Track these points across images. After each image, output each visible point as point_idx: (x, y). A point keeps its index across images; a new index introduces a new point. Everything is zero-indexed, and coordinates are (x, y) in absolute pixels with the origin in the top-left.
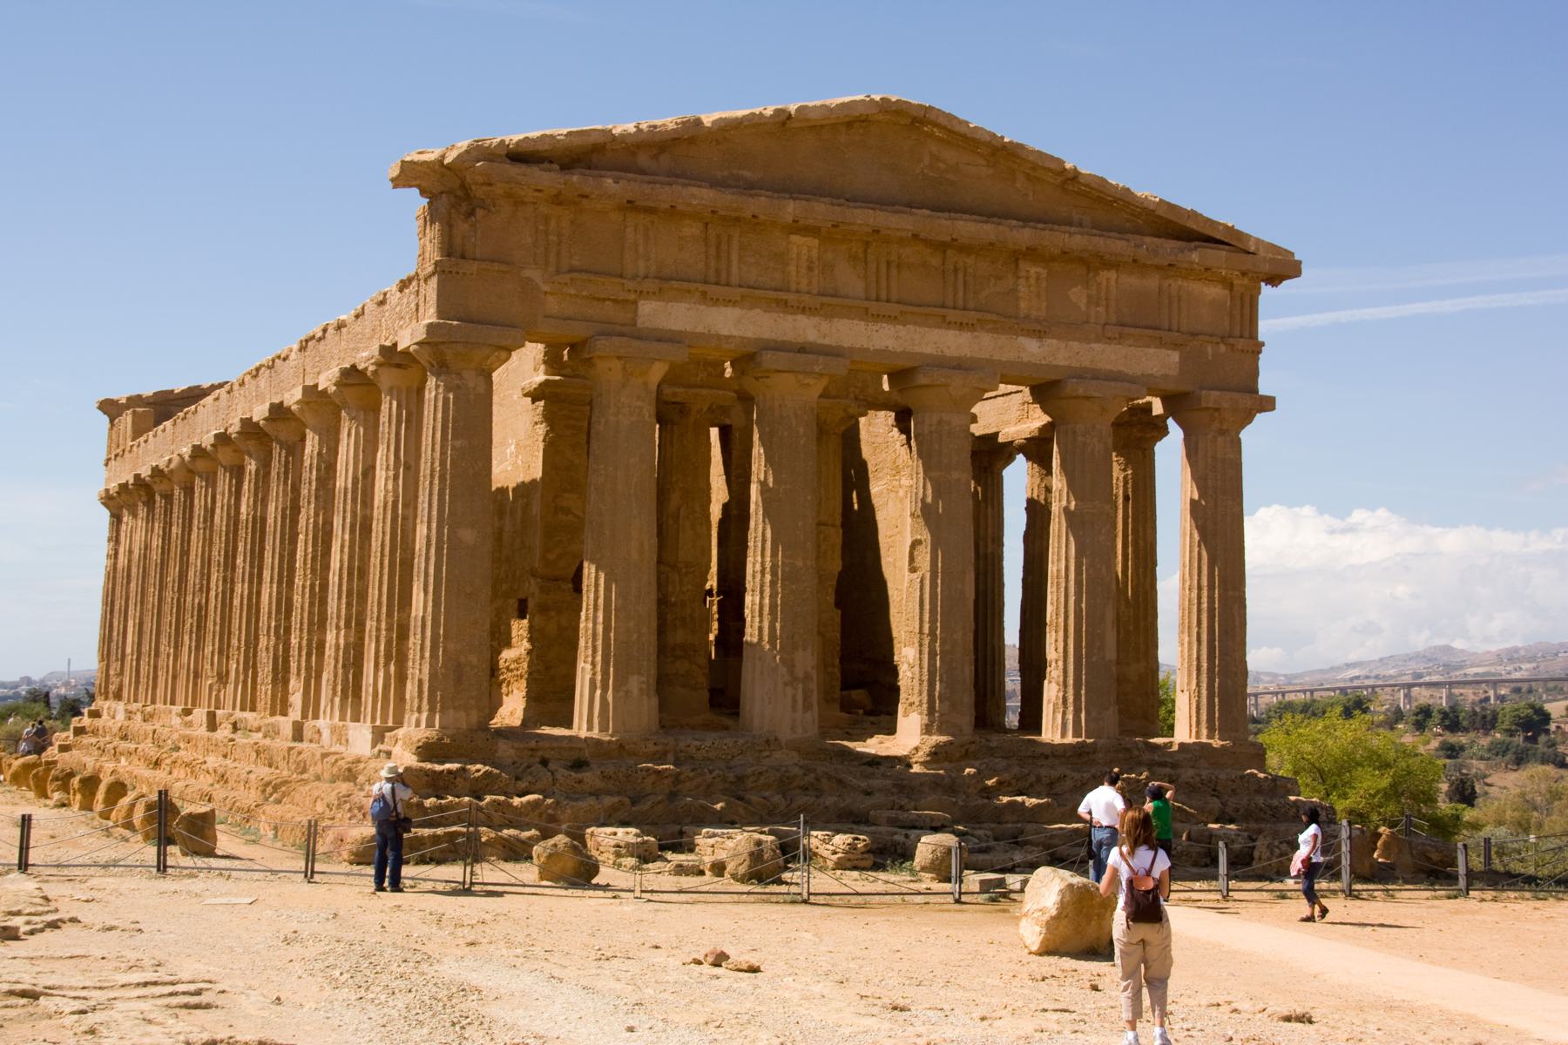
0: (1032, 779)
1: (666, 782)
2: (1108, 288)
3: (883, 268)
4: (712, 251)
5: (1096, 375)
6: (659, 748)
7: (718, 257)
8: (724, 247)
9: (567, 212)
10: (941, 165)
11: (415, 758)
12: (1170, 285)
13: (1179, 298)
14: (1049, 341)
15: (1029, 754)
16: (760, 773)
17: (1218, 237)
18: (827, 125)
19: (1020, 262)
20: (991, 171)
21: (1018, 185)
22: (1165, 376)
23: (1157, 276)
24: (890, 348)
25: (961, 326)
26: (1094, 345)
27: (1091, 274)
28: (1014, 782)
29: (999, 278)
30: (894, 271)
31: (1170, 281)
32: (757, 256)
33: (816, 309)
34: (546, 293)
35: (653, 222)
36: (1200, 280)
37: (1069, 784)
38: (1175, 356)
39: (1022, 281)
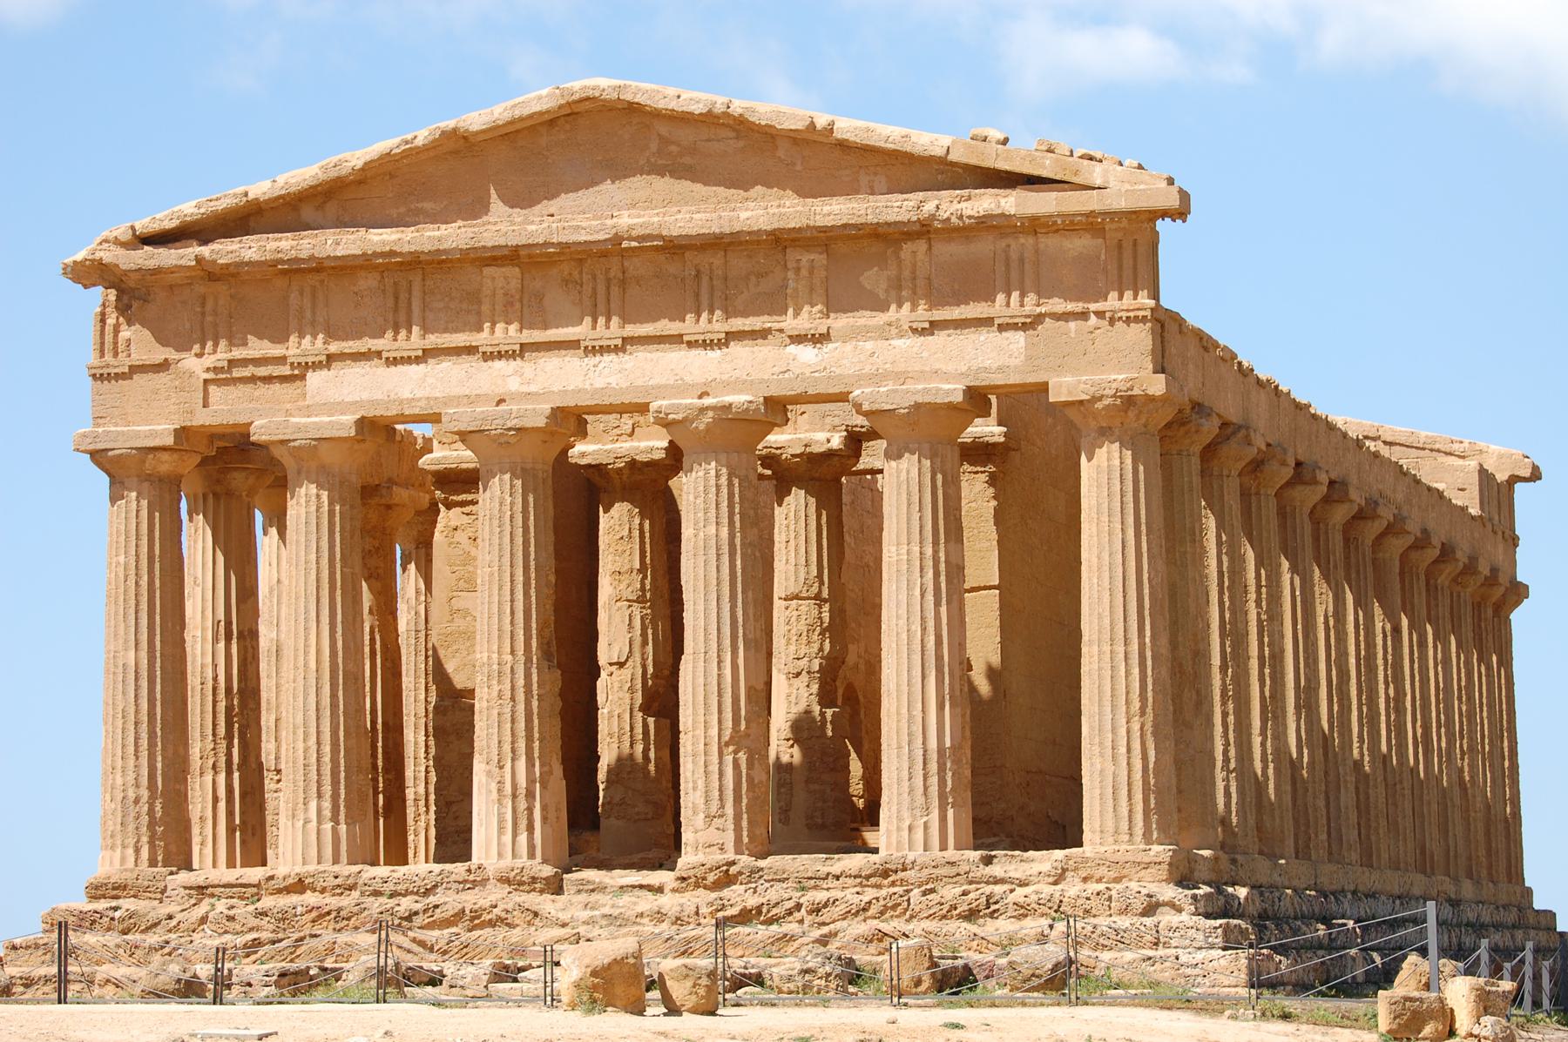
0: (789, 905)
1: (328, 918)
2: (914, 265)
3: (601, 289)
4: (390, 302)
5: (903, 377)
7: (396, 310)
8: (403, 296)
9: (225, 288)
10: (673, 148)
11: (86, 900)
12: (1009, 246)
13: (1022, 260)
14: (831, 346)
15: (810, 874)
16: (436, 907)
17: (1045, 174)
18: (523, 129)
19: (788, 250)
20: (741, 144)
21: (781, 153)
22: (1000, 369)
23: (991, 238)
24: (614, 385)
25: (707, 345)
26: (892, 342)
27: (889, 251)
28: (764, 910)
29: (760, 275)
30: (615, 290)
31: (1010, 241)
32: (446, 299)
33: (514, 351)
34: (206, 381)
35: (322, 282)
36: (1057, 231)
37: (840, 909)
38: (1018, 339)
39: (791, 275)
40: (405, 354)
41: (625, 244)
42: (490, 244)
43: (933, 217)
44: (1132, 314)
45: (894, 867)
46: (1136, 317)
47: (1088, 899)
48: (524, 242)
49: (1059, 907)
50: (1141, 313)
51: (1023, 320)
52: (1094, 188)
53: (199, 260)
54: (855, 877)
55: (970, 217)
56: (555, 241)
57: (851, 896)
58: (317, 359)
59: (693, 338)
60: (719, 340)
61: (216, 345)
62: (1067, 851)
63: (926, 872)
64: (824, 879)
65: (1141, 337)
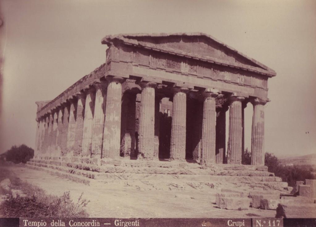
38: (253, 90)
48: (194, 56)
53: (139, 45)
56: (199, 58)
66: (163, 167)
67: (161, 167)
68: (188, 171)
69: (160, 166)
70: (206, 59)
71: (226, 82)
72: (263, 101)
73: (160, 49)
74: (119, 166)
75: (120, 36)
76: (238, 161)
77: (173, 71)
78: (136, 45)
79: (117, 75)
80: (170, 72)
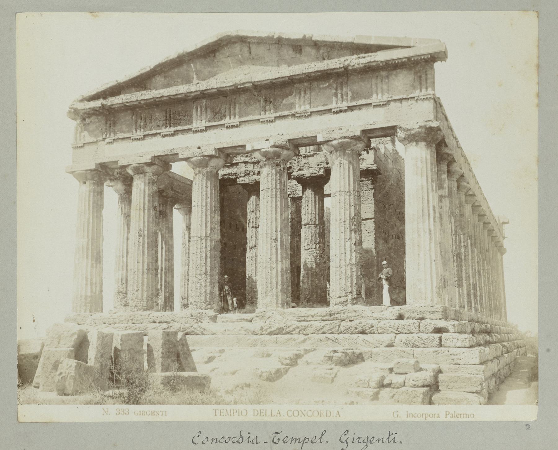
0: (294, 326)
6: (142, 317)
15: (302, 315)
33: (203, 130)
40: (168, 133)
41: (239, 87)
42: (193, 90)
43: (348, 65)
44: (425, 97)
45: (334, 313)
46: (427, 98)
47: (409, 325)
48: (205, 88)
49: (398, 329)
50: (429, 96)
51: (383, 103)
52: (410, 47)
53: (103, 105)
54: (319, 316)
55: (362, 64)
57: (318, 324)
58: (140, 137)
59: (263, 120)
60: (272, 120)
61: (110, 135)
62: (400, 307)
63: (346, 314)
64: (308, 317)
65: (429, 106)
66: (159, 323)
67: (154, 322)
68: (198, 329)
69: (152, 320)
70: (231, 84)
71: (296, 115)
72: (413, 132)
73: (137, 100)
74: (83, 324)
75: (75, 103)
76: (340, 297)
77: (174, 131)
78: (100, 107)
79: (76, 170)
80: (139, 139)
